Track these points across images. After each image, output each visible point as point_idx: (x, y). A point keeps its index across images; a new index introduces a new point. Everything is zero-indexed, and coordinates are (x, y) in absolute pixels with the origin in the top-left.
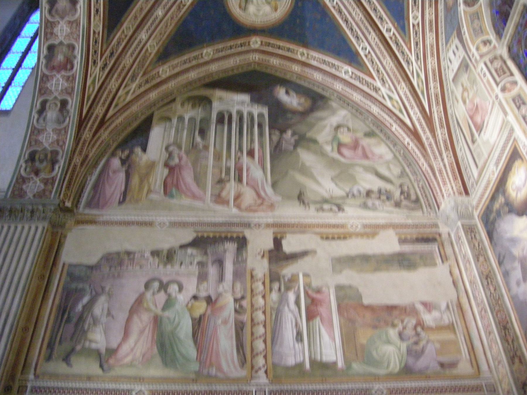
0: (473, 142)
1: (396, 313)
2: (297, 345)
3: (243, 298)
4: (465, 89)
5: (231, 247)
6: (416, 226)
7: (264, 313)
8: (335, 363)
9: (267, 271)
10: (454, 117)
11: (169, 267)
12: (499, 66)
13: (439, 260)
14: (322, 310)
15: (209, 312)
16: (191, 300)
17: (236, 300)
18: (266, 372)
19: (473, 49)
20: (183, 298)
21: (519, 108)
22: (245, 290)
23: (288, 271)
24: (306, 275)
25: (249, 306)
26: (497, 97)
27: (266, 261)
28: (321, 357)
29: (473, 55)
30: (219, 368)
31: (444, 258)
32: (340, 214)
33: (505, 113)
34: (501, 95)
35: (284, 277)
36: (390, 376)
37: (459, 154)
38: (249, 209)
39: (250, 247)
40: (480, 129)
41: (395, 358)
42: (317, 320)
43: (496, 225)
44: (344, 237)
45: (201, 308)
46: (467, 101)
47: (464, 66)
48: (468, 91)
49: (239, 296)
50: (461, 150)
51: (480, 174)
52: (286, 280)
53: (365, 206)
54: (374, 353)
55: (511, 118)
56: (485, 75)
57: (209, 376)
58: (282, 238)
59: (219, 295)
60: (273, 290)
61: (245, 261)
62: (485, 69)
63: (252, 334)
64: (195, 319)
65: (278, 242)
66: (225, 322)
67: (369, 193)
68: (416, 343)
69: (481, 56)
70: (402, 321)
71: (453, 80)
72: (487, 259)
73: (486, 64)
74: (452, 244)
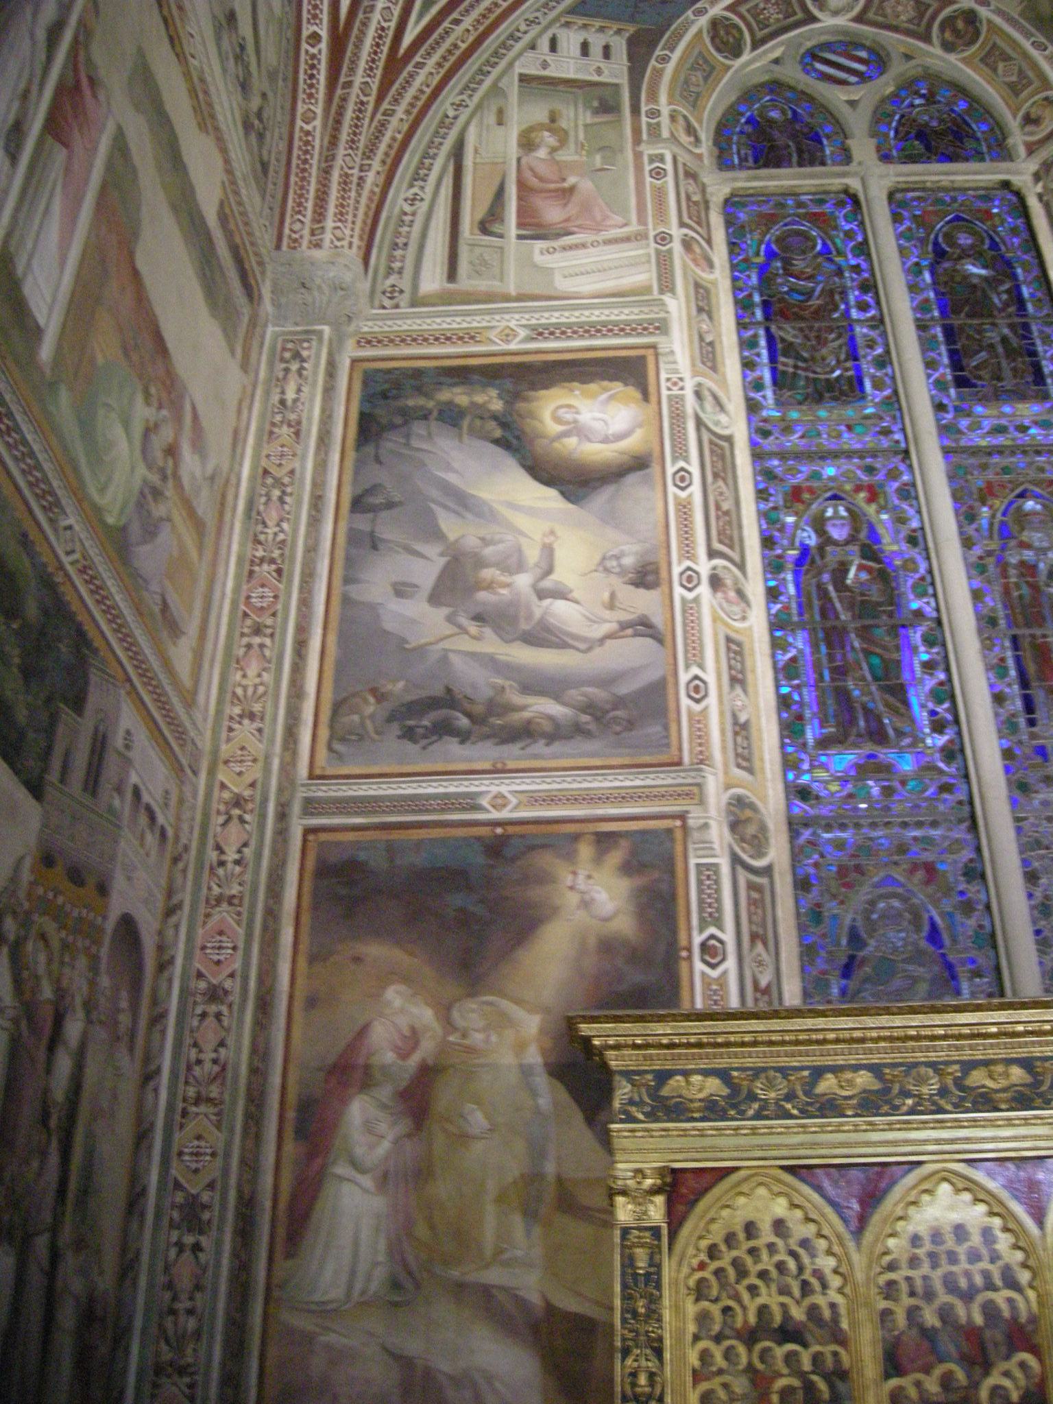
21: (700, 310)
34: (677, 247)
40: (534, 229)
43: (418, 428)
46: (542, 153)
69: (674, 138)
71: (523, 79)
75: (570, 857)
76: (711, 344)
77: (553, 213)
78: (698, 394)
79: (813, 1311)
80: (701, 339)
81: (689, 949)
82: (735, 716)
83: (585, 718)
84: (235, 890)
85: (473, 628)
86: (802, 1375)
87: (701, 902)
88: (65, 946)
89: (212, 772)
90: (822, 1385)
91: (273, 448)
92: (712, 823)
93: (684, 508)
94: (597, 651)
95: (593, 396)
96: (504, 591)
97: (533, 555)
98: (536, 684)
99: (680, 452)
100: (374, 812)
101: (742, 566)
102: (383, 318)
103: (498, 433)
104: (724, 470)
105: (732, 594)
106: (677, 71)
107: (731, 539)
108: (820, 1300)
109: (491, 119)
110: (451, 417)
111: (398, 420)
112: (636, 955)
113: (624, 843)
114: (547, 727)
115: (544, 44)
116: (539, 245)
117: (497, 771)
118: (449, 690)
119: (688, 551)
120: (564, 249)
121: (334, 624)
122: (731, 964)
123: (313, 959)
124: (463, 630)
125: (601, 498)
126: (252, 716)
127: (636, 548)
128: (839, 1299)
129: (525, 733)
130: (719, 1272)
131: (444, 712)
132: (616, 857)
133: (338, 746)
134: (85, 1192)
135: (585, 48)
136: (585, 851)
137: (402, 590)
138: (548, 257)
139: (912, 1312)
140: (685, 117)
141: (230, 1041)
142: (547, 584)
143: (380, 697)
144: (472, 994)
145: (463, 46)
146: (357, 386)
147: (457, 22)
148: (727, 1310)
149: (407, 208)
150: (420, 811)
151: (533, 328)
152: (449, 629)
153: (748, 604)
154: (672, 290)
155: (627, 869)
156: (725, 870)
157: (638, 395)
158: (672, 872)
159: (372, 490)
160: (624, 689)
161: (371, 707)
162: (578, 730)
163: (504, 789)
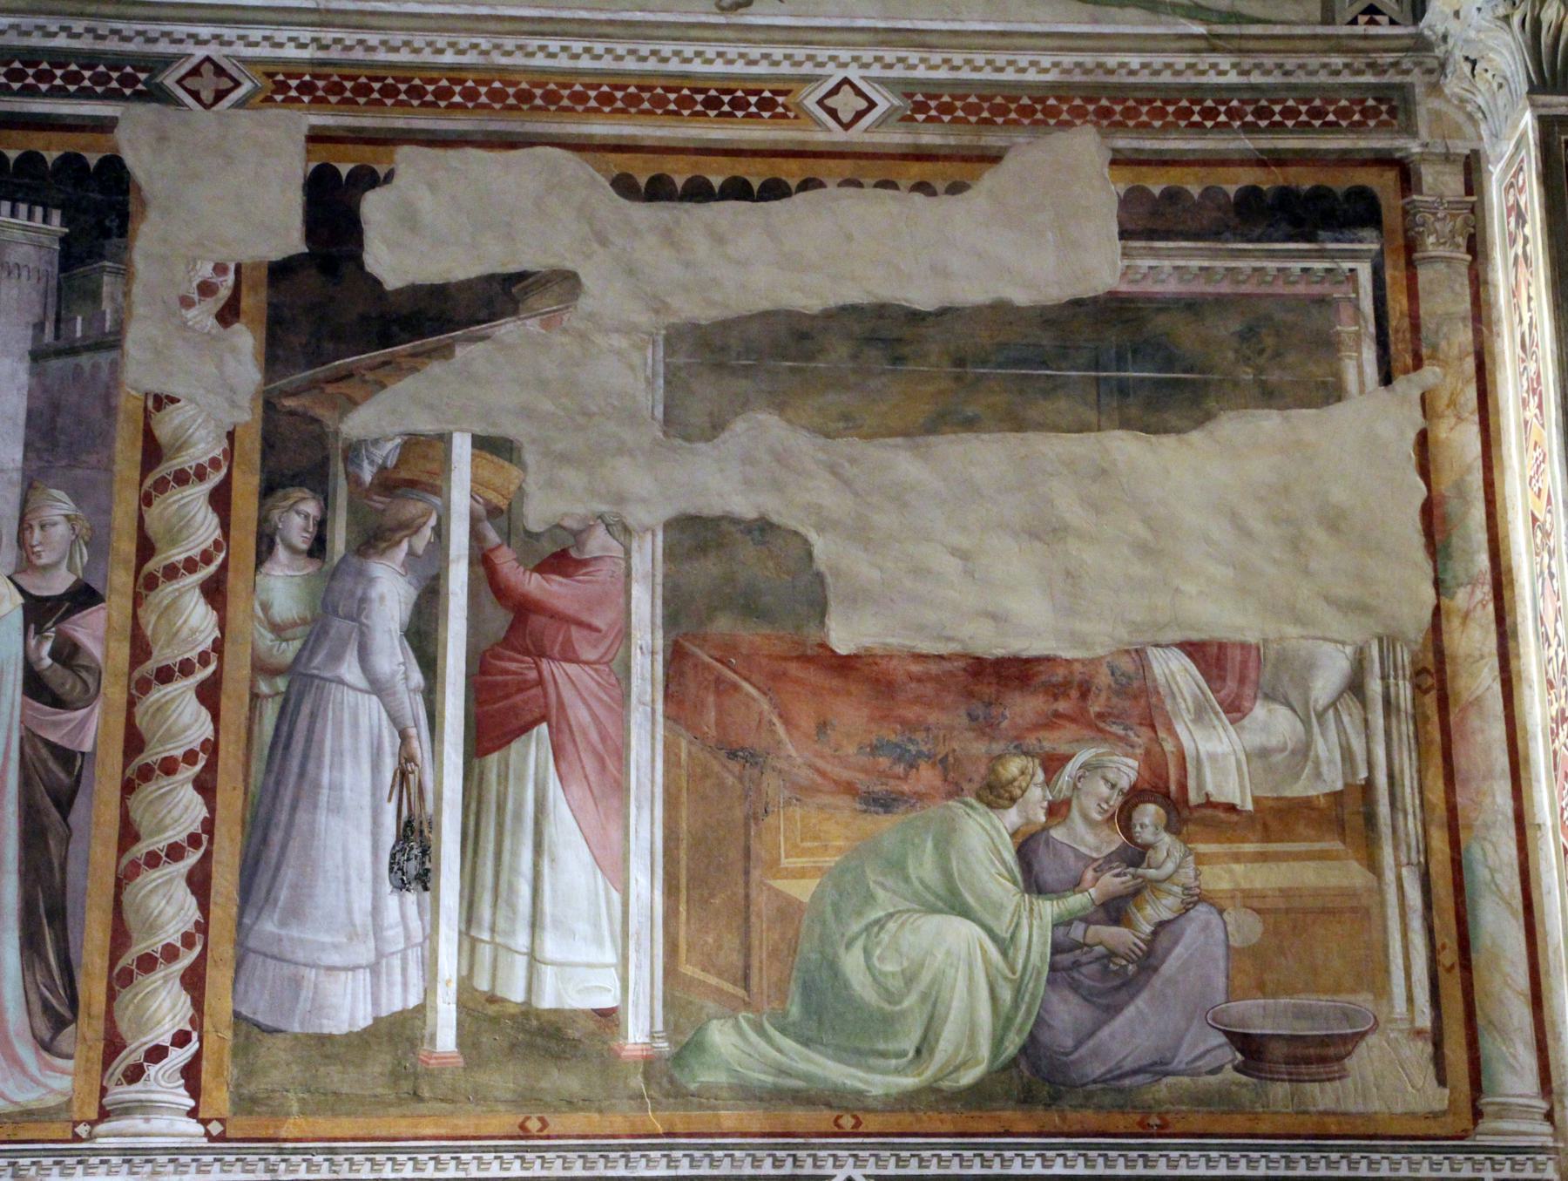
1: (1024, 707)
2: (392, 901)
3: (84, 596)
7: (209, 695)
9: (247, 415)
17: (38, 612)
18: (191, 1075)
22: (98, 544)
24: (490, 446)
25: (122, 652)
27: (245, 340)
28: (529, 989)
35: (353, 452)
39: (147, 238)
41: (971, 1009)
42: (534, 749)
49: (59, 583)
52: (367, 474)
54: (852, 963)
60: (281, 553)
61: (111, 342)
63: (128, 834)
68: (1115, 910)
70: (1053, 764)
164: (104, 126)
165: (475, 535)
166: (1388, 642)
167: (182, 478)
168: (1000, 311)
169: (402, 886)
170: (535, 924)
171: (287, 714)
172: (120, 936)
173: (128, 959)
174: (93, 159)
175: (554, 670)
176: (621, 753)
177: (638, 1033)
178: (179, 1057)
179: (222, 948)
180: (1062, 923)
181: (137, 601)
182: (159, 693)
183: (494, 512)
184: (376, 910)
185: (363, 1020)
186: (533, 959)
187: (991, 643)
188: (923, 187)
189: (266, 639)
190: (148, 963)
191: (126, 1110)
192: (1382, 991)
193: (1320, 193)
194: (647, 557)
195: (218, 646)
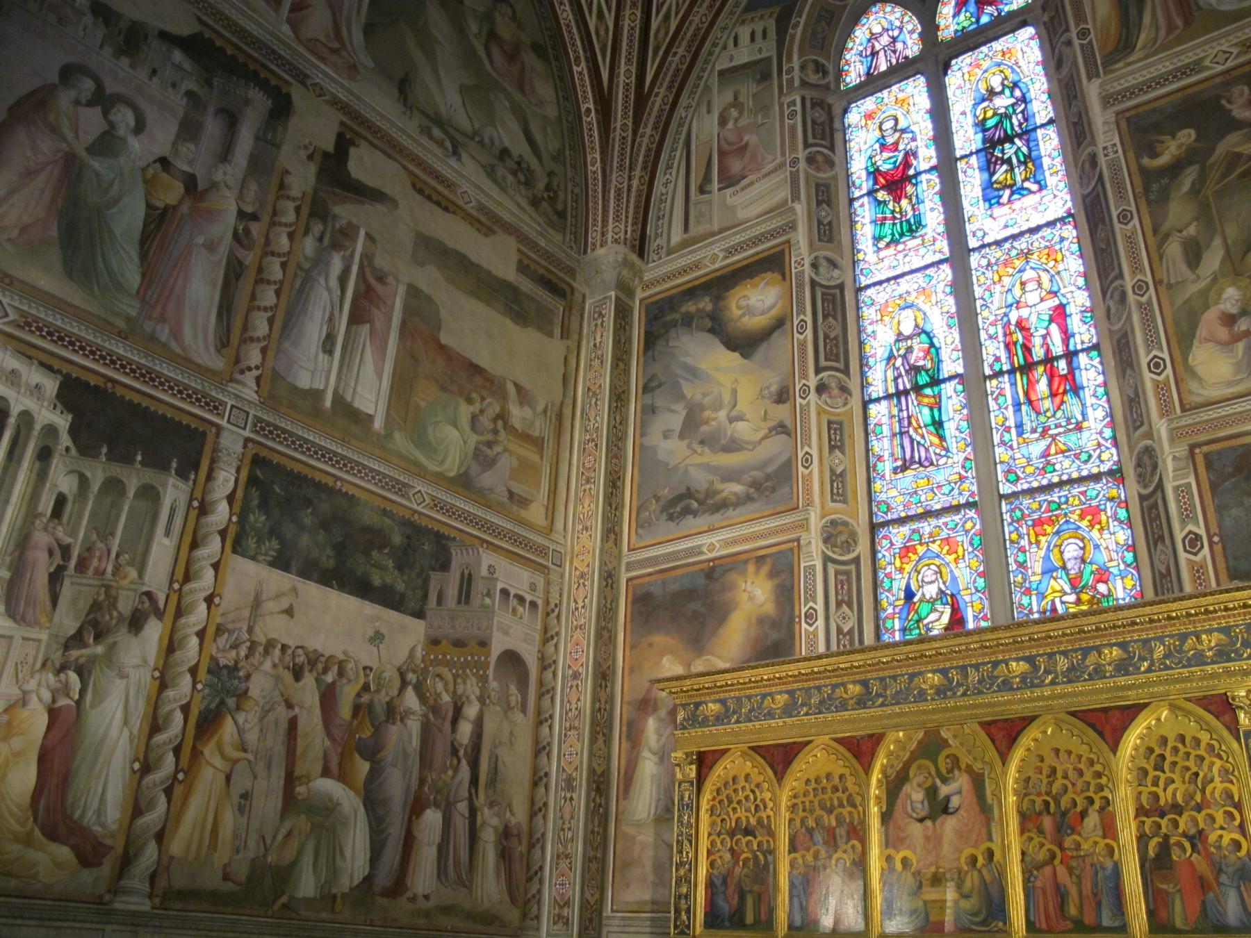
0: (702, 190)
1: (478, 380)
2: (321, 355)
3: (254, 217)
4: (736, 104)
5: (259, 102)
6: (548, 256)
8: (370, 418)
9: (310, 190)
10: (686, 126)
11: (125, 61)
12: (819, 121)
13: (557, 332)
14: (377, 314)
15: (185, 208)
16: (155, 162)
17: (241, 215)
18: (258, 380)
19: (796, 63)
20: (139, 149)
21: (819, 203)
23: (345, 212)
24: (369, 236)
25: (262, 240)
26: (795, 162)
27: (312, 169)
29: (790, 70)
30: (177, 334)
31: (565, 334)
32: (452, 162)
33: (795, 196)
34: (802, 165)
36: (440, 479)
37: (658, 187)
38: (312, 45)
39: (294, 121)
40: (728, 181)
42: (365, 329)
43: (673, 333)
44: (447, 206)
45: (171, 193)
46: (730, 125)
47: (760, 71)
48: (741, 113)
50: (666, 185)
51: (684, 244)
52: (337, 226)
53: (491, 172)
54: (430, 430)
55: (800, 209)
56: (793, 114)
57: (153, 338)
58: (353, 143)
59: (214, 186)
61: (278, 146)
62: (798, 108)
64: (155, 208)
65: (343, 144)
66: (211, 247)
67: (504, 153)
68: (489, 444)
69: (804, 84)
70: (483, 399)
71: (722, 73)
72: (627, 372)
73: (803, 99)
74: (582, 316)
75: (744, 573)
76: (830, 223)
77: (736, 166)
78: (814, 266)
79: (760, 821)
80: (820, 223)
81: (800, 617)
82: (832, 470)
83: (752, 490)
84: (583, 621)
85: (699, 449)
86: (754, 852)
87: (806, 588)
88: (455, 677)
89: (571, 563)
90: (761, 857)
91: (591, 375)
92: (813, 541)
93: (803, 345)
94: (758, 448)
95: (755, 286)
96: (713, 423)
97: (727, 398)
98: (730, 476)
99: (802, 310)
100: (657, 564)
101: (846, 371)
102: (656, 267)
103: (709, 325)
104: (834, 309)
105: (836, 392)
106: (804, 30)
107: (837, 355)
108: (764, 815)
109: (704, 109)
110: (687, 321)
111: (662, 331)
112: (775, 624)
113: (769, 560)
114: (733, 498)
115: (731, 43)
116: (729, 191)
117: (711, 530)
118: (688, 489)
119: (804, 375)
120: (742, 189)
121: (637, 461)
122: (820, 622)
123: (633, 647)
124: (695, 451)
125: (760, 353)
126: (587, 529)
127: (777, 379)
128: (771, 813)
129: (723, 506)
130: (720, 802)
131: (688, 501)
132: (765, 569)
133: (640, 531)
134: (492, 782)
135: (753, 35)
136: (751, 568)
137: (666, 435)
138: (734, 198)
139: (803, 821)
140: (815, 62)
141: (582, 698)
142: (734, 413)
143: (657, 499)
144: (699, 656)
145: (684, 67)
146: (643, 314)
147: (675, 54)
148: (723, 820)
149: (664, 191)
150: (679, 559)
151: (726, 250)
152: (688, 452)
153: (850, 394)
154: (799, 199)
155: (772, 575)
156: (819, 568)
157: (780, 277)
158: (792, 573)
159: (653, 377)
160: (770, 469)
161: (654, 506)
162: (749, 498)
163: (713, 540)
164: (290, 84)
165: (361, 260)
166: (553, 404)
167: (288, 198)
168: (489, 273)
169: (324, 352)
170: (357, 381)
171: (303, 285)
172: (245, 328)
173: (246, 335)
174: (284, 91)
175: (375, 311)
176: (386, 342)
177: (378, 424)
178: (255, 373)
179: (273, 346)
180: (478, 442)
181: (270, 227)
182: (270, 258)
183: (367, 256)
184: (317, 355)
185: (307, 387)
186: (355, 391)
187: (475, 360)
188: (478, 230)
189: (302, 259)
190: (252, 339)
191: (239, 382)
192: (539, 491)
193: (556, 285)
194: (402, 290)
195: (289, 253)
